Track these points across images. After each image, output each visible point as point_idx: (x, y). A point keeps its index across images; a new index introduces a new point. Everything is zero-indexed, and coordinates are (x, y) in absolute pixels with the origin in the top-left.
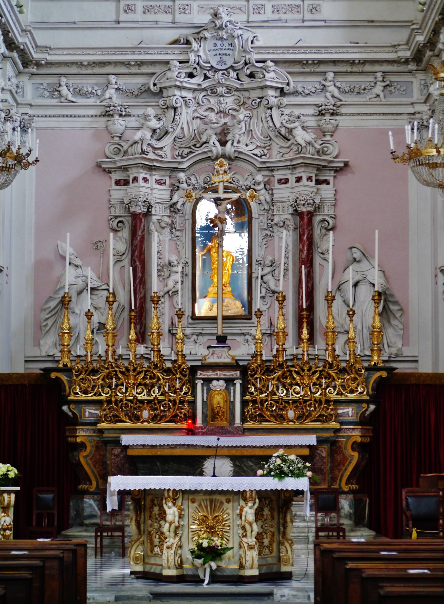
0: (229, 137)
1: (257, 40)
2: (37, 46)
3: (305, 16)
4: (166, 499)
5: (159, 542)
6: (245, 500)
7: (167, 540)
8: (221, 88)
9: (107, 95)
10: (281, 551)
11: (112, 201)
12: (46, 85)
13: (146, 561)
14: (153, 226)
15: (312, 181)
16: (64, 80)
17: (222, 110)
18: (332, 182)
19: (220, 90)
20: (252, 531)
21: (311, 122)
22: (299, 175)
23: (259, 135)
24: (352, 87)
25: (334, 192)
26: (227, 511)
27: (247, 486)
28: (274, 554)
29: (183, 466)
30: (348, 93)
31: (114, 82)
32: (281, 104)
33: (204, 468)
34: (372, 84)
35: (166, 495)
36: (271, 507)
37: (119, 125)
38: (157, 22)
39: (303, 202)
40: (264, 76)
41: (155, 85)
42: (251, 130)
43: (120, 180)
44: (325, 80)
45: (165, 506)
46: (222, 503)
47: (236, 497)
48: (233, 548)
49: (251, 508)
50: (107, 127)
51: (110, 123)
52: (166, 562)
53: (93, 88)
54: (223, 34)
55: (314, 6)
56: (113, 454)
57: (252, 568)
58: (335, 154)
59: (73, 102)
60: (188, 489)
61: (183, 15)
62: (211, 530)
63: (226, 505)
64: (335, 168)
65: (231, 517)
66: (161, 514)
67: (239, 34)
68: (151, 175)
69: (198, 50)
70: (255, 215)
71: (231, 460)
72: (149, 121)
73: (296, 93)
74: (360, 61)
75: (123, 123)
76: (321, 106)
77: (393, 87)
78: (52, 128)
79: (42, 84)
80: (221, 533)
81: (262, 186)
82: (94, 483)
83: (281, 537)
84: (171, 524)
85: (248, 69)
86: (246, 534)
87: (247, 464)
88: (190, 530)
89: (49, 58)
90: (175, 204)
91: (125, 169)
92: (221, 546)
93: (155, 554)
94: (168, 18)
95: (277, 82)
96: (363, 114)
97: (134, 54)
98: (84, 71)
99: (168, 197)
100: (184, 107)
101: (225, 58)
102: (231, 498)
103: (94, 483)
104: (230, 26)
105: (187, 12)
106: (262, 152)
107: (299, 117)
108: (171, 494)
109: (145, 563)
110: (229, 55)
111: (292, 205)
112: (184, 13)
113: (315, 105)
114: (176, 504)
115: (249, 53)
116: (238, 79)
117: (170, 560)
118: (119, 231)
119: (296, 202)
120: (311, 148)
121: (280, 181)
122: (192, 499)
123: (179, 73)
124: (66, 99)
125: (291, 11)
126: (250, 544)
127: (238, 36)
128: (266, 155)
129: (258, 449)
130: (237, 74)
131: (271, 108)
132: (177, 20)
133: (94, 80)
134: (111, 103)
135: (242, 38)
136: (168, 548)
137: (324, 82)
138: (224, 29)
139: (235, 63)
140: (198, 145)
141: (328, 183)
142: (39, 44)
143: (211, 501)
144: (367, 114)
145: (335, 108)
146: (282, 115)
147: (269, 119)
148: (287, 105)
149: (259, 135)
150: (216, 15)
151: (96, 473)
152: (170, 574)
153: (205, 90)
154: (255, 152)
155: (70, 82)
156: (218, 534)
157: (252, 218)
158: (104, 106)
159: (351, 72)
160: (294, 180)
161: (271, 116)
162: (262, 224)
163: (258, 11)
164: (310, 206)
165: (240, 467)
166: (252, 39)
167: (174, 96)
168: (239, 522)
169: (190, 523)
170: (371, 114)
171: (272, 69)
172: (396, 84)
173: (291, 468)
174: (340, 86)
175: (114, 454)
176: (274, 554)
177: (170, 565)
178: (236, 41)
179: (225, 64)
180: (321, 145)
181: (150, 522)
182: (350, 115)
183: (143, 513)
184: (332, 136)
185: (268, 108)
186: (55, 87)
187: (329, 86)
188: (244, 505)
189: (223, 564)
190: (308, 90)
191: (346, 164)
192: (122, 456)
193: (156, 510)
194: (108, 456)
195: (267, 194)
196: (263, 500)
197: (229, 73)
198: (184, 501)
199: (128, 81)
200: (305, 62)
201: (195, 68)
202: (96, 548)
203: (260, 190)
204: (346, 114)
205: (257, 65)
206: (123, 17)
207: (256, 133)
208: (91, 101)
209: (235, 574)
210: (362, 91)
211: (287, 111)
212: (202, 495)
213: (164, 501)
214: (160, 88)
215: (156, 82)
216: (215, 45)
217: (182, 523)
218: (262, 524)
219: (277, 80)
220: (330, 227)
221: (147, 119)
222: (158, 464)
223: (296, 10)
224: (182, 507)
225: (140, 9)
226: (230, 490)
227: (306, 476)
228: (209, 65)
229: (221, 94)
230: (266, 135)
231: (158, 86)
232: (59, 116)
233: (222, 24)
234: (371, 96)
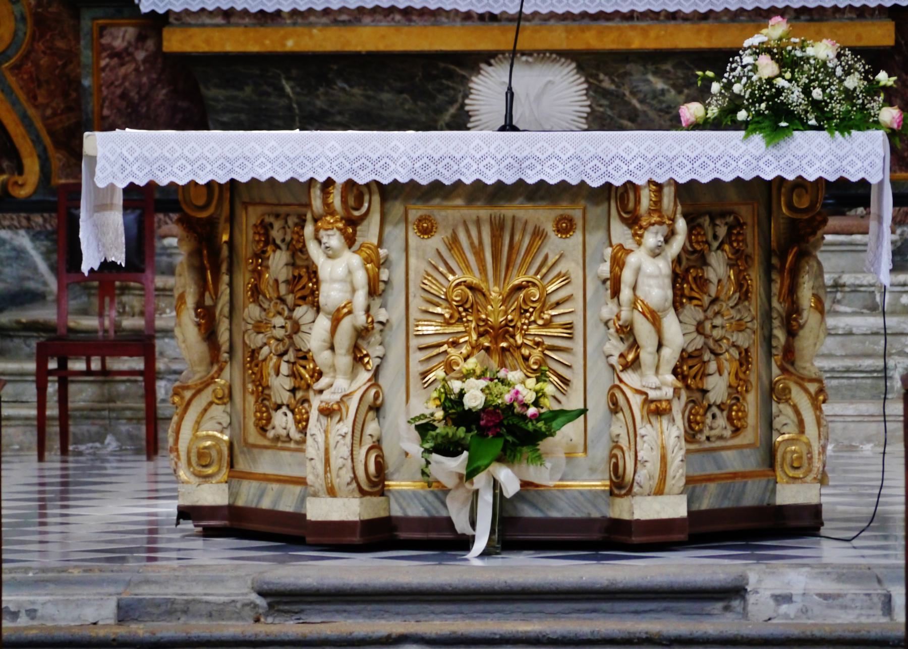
4: (315, 220)
5: (293, 391)
6: (633, 221)
7: (323, 382)
10: (777, 424)
13: (242, 465)
20: (660, 346)
26: (561, 268)
27: (640, 167)
28: (748, 436)
29: (386, 96)
33: (471, 104)
35: (317, 204)
36: (736, 252)
45: (313, 249)
46: (539, 234)
47: (596, 212)
48: (584, 411)
49: (656, 253)
52: (320, 468)
56: (103, 48)
57: (659, 491)
60: (403, 179)
62: (496, 339)
63: (554, 244)
65: (575, 289)
66: (296, 279)
71: (580, 69)
80: (536, 354)
82: (32, 167)
83: (775, 370)
84: (336, 319)
86: (637, 357)
87: (644, 88)
88: (414, 343)
92: (536, 403)
93: (277, 438)
102: (577, 214)
103: (32, 167)
108: (336, 199)
109: (235, 475)
114: (359, 240)
117: (335, 463)
122: (420, 220)
126: (652, 394)
129: (687, 26)
136: (327, 412)
143: (498, 228)
151: (39, 125)
152: (335, 517)
156: (526, 359)
165: (615, 98)
168: (608, 310)
169: (414, 314)
173: (817, 94)
175: (110, 47)
176: (748, 436)
177: (336, 482)
181: (253, 311)
183: (226, 278)
188: (629, 244)
189: (541, 475)
192: (141, 55)
193: (278, 262)
194: (86, 56)
196: (706, 221)
198: (388, 229)
202: (42, 418)
209: (595, 514)
212: (459, 202)
213: (309, 230)
217: (382, 315)
218: (700, 316)
222: (288, 89)
224: (383, 252)
226: (574, 181)
227: (877, 124)
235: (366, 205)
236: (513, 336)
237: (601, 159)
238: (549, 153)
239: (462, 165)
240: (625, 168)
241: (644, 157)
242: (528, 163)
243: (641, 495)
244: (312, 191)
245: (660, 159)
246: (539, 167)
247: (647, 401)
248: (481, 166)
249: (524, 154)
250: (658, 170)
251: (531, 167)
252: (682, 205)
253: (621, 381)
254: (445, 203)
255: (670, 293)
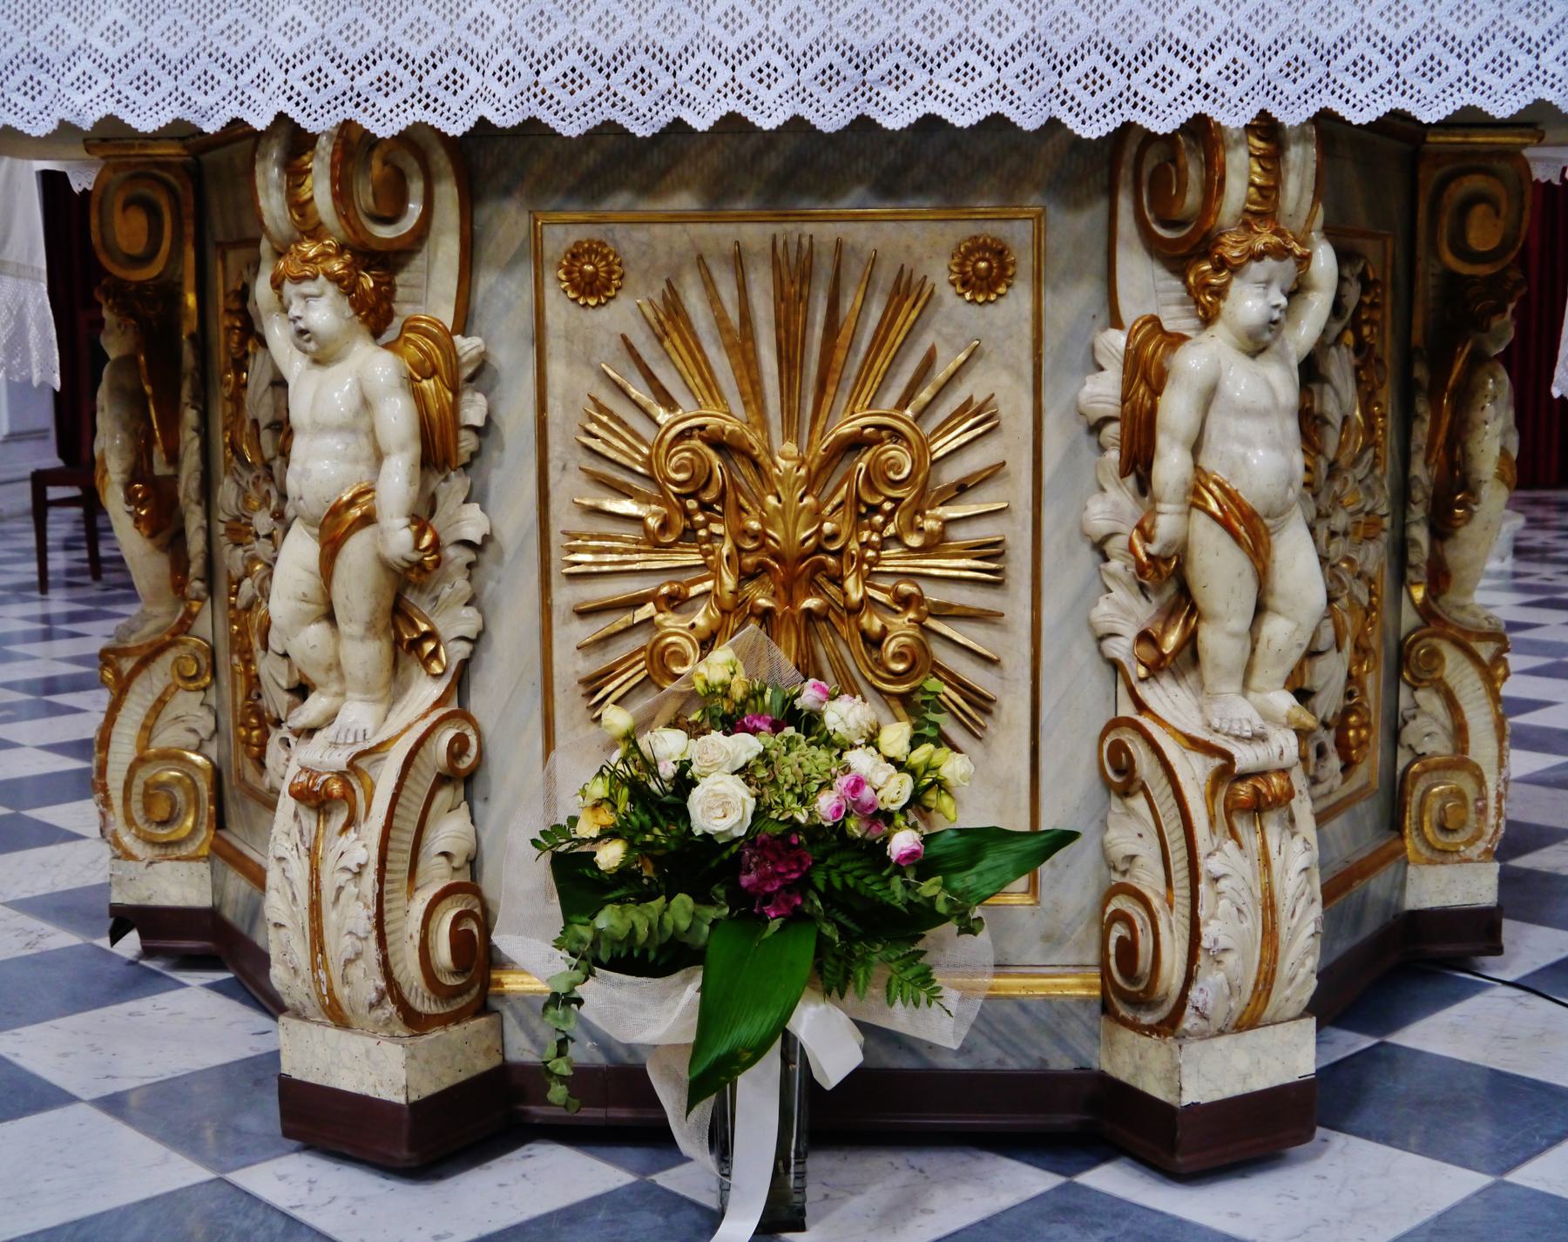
26: (973, 387)
27: (1234, 72)
28: (1365, 772)
49: (1256, 345)
57: (1248, 1021)
62: (788, 591)
65: (1012, 447)
80: (901, 627)
86: (1190, 640)
88: (565, 596)
102: (1017, 235)
117: (339, 946)
126: (1246, 758)
136: (316, 800)
152: (348, 1081)
156: (874, 642)
169: (564, 518)
177: (343, 993)
183: (191, 416)
188: (1176, 319)
198: (486, 281)
209: (1061, 1062)
213: (262, 289)
217: (472, 524)
224: (467, 346)
235: (415, 208)
236: (838, 580)
237: (1113, 56)
238: (950, 32)
239: (683, 75)
240: (1189, 76)
241: (1248, 45)
242: (885, 65)
243: (1203, 1036)
244: (258, 168)
245: (1296, 48)
246: (921, 77)
247: (1226, 774)
248: (742, 74)
249: (876, 37)
250: (1286, 86)
251: (897, 77)
252: (1325, 206)
253: (1141, 706)
254: (647, 205)
255: (1298, 460)
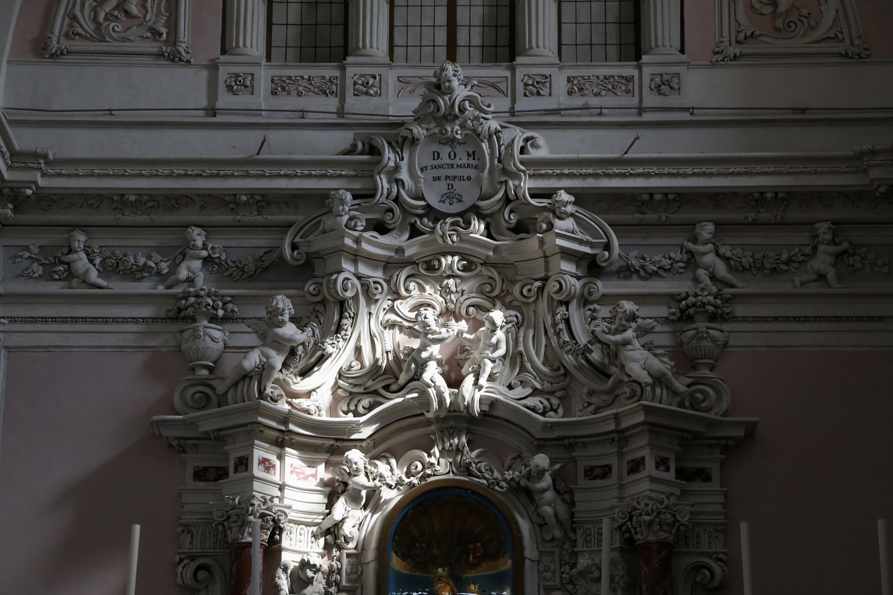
0: (467, 368)
1: (532, 146)
2: (14, 154)
3: (644, 100)
8: (450, 258)
9: (183, 273)
11: (186, 519)
12: (37, 251)
14: (283, 576)
15: (667, 470)
16: (80, 239)
17: (452, 306)
18: (716, 474)
19: (446, 261)
21: (663, 339)
22: (637, 455)
23: (539, 363)
24: (757, 256)
25: (721, 499)
30: (750, 269)
31: (199, 243)
32: (590, 294)
34: (808, 250)
37: (207, 339)
38: (303, 112)
39: (647, 518)
40: (551, 226)
41: (294, 247)
42: (521, 354)
43: (206, 469)
44: (695, 240)
50: (179, 346)
51: (186, 335)
53: (149, 258)
54: (455, 130)
55: (665, 77)
58: (724, 406)
59: (100, 287)
61: (364, 98)
64: (723, 442)
67: (493, 129)
68: (281, 457)
69: (397, 168)
70: (530, 551)
72: (281, 324)
73: (626, 272)
74: (776, 194)
75: (217, 334)
76: (686, 298)
77: (857, 258)
78: (47, 348)
79: (27, 248)
81: (546, 481)
85: (511, 212)
89: (41, 182)
90: (338, 525)
91: (218, 438)
94: (332, 103)
95: (581, 242)
96: (786, 319)
97: (248, 176)
98: (129, 218)
99: (322, 508)
100: (362, 301)
101: (459, 186)
104: (470, 110)
105: (372, 92)
106: (546, 403)
107: (633, 317)
110: (469, 178)
111: (620, 527)
112: (367, 93)
113: (672, 296)
115: (515, 176)
116: (489, 236)
118: (199, 590)
119: (631, 519)
120: (665, 392)
121: (590, 473)
123: (351, 218)
124: (84, 282)
125: (613, 91)
127: (490, 136)
128: (556, 411)
130: (487, 227)
131: (567, 304)
132: (348, 107)
133: (152, 240)
134: (191, 290)
135: (498, 139)
137: (690, 245)
138: (456, 117)
139: (482, 198)
140: (394, 387)
141: (708, 478)
142: (17, 148)
144: (796, 319)
145: (719, 302)
146: (594, 318)
147: (562, 326)
148: (604, 295)
149: (539, 363)
150: (438, 87)
153: (411, 262)
154: (531, 402)
155: (96, 245)
157: (523, 559)
158: (174, 296)
159: (755, 223)
160: (625, 468)
161: (567, 322)
162: (548, 575)
163: (535, 91)
164: (665, 528)
166: (521, 144)
167: (339, 272)
170: (806, 319)
171: (570, 209)
172: (864, 249)
174: (729, 254)
178: (485, 146)
179: (460, 201)
180: (689, 386)
182: (755, 319)
184: (712, 369)
185: (561, 303)
186: (59, 254)
187: (704, 254)
190: (654, 263)
191: (751, 430)
195: (559, 502)
197: (468, 224)
199: (234, 243)
200: (646, 197)
201: (391, 210)
203: (544, 491)
204: (745, 319)
205: (533, 202)
206: (225, 100)
207: (530, 360)
208: (143, 287)
210: (782, 267)
211: (604, 311)
214: (307, 254)
215: (297, 239)
216: (437, 155)
219: (579, 236)
220: (716, 583)
221: (275, 320)
223: (623, 88)
225: (263, 83)
228: (423, 203)
229: (448, 273)
230: (556, 365)
231: (303, 249)
232: (64, 320)
233: (453, 105)
234: (805, 277)
